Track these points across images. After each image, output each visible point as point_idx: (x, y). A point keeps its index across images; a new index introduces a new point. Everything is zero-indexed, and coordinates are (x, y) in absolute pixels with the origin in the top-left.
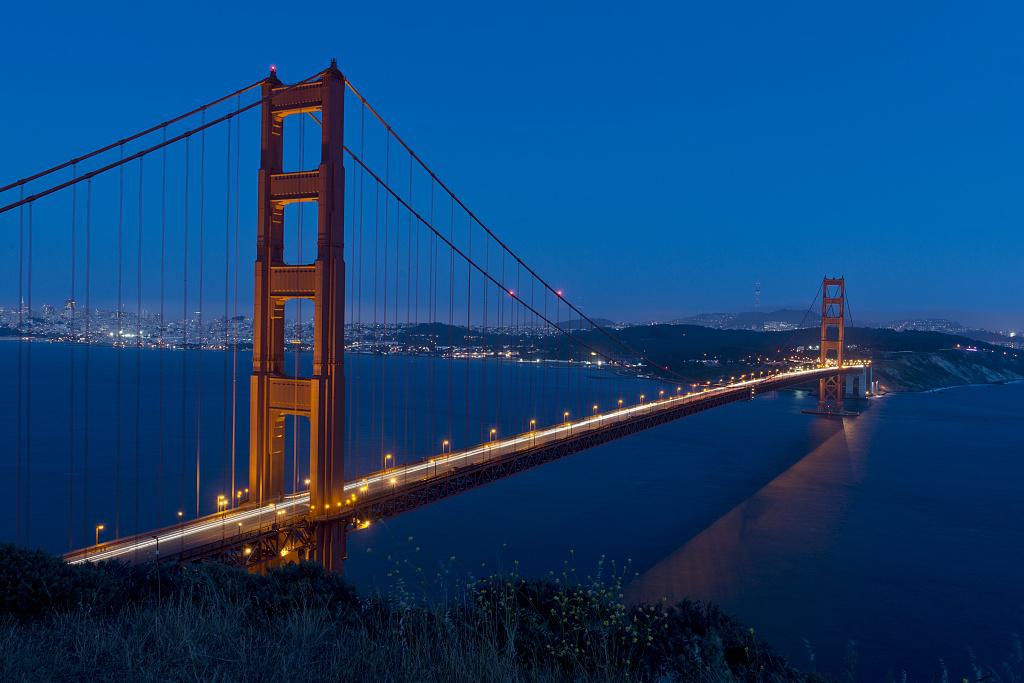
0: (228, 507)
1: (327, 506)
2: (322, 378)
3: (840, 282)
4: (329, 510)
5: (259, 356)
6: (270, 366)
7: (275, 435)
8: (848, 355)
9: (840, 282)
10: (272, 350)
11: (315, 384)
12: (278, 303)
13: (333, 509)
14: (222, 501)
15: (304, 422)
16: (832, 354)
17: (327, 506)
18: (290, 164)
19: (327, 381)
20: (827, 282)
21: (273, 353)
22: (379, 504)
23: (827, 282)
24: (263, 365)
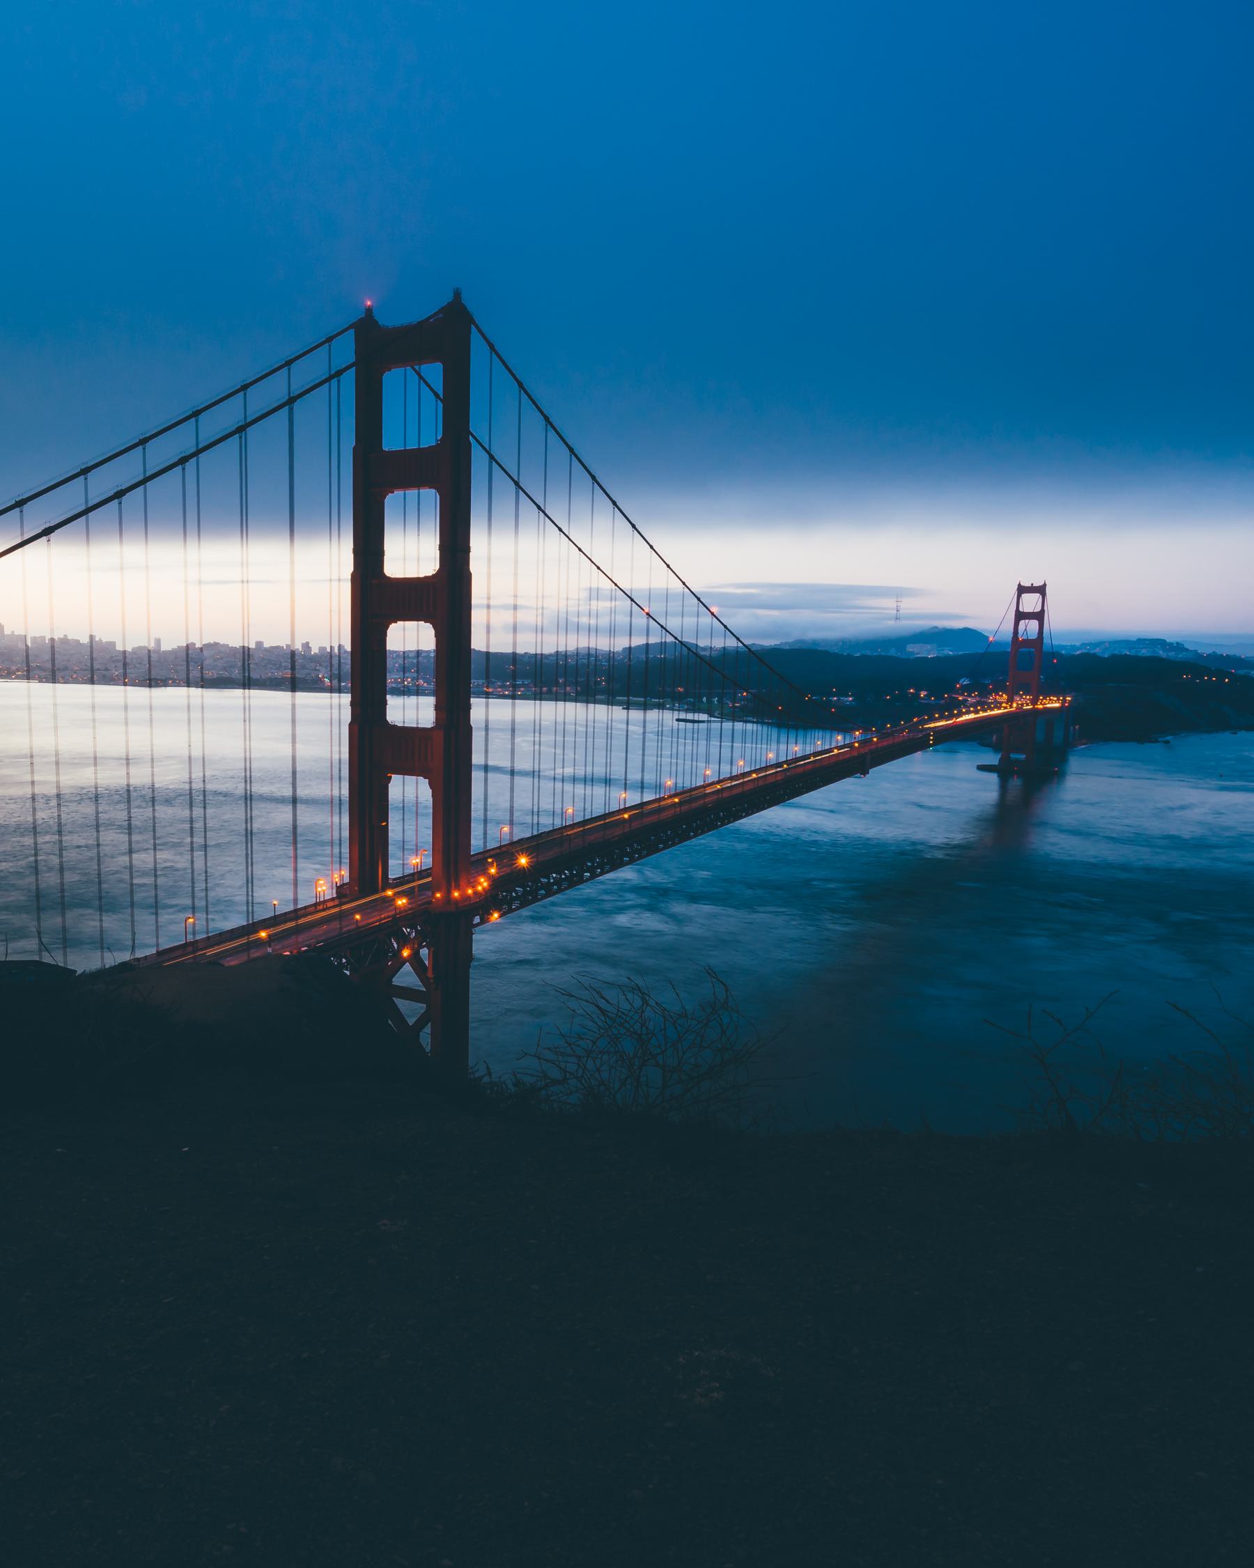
1: (456, 894)
3: (1041, 590)
4: (456, 901)
9: (1041, 590)
13: (465, 897)
18: (392, 441)
20: (1022, 590)
23: (1022, 590)
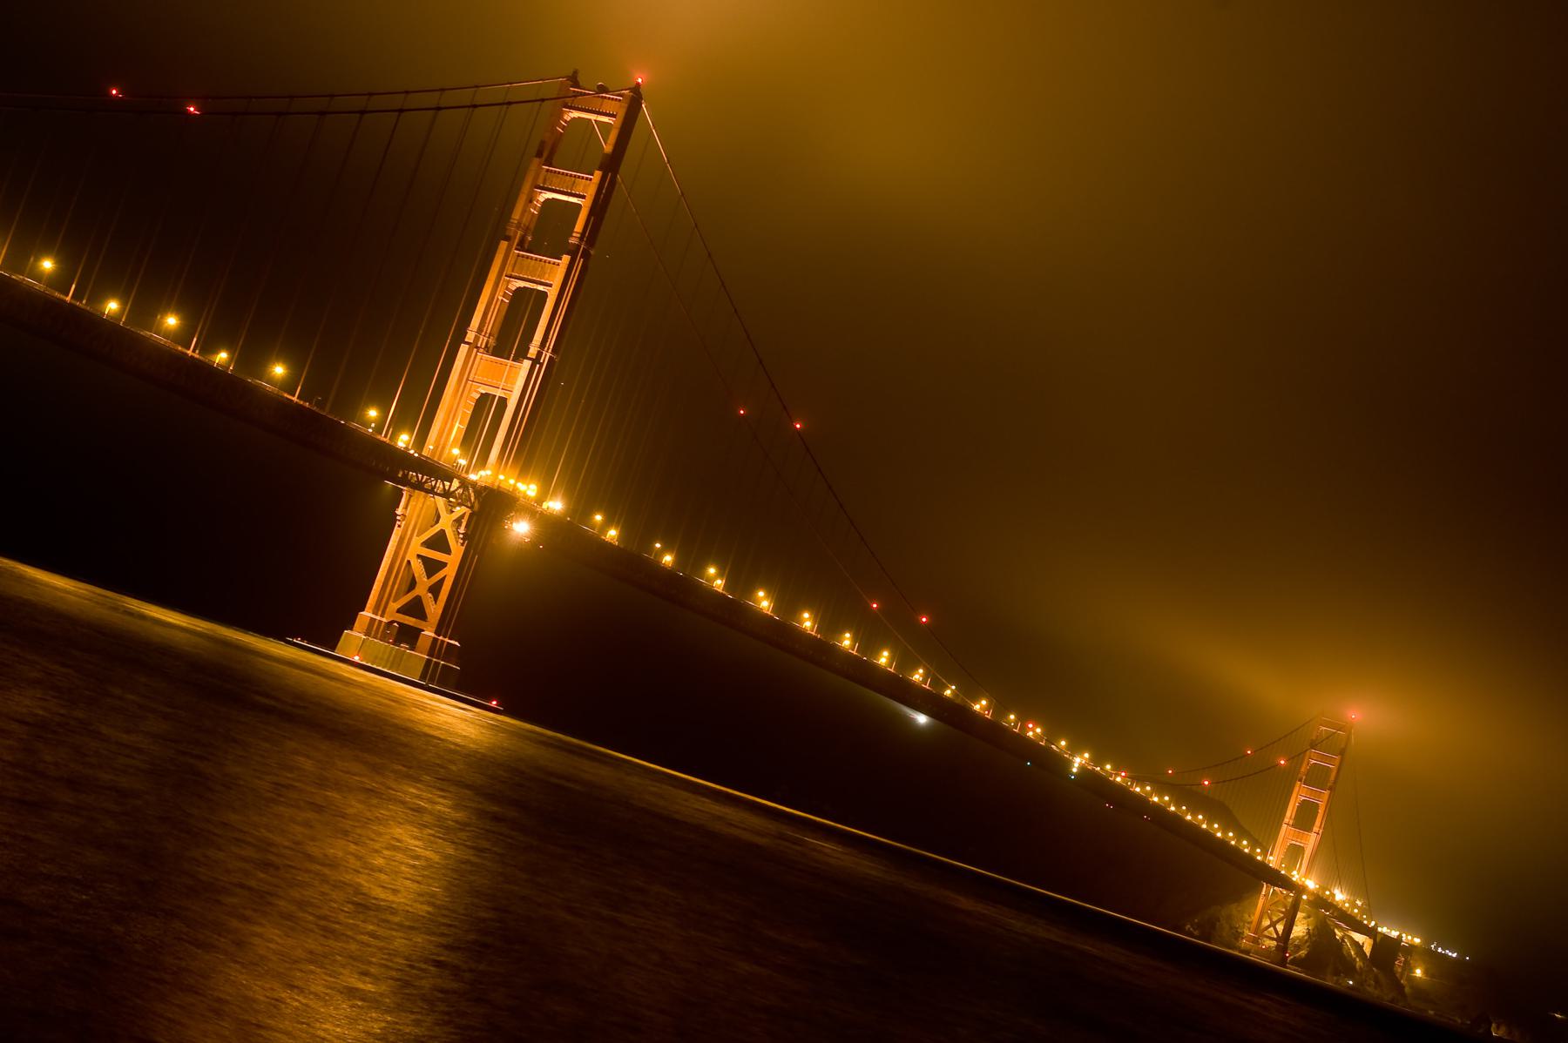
5: (477, 326)
6: (482, 341)
7: (467, 411)
11: (527, 364)
15: (503, 402)
19: (538, 366)
21: (488, 332)
24: (476, 338)
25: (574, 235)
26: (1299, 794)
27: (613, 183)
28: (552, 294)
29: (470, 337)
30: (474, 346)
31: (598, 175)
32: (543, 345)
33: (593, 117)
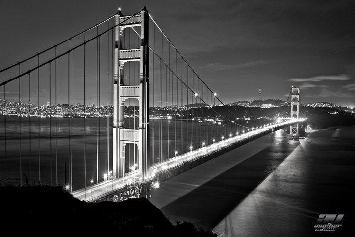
0: (107, 179)
2: (143, 129)
6: (120, 124)
7: (122, 151)
8: (300, 116)
10: (121, 118)
12: (123, 100)
14: (105, 176)
15: (136, 145)
16: (295, 116)
17: (146, 178)
22: (161, 177)
24: (118, 124)
25: (141, 74)
26: (293, 104)
27: (148, 49)
28: (140, 99)
29: (115, 124)
30: (118, 127)
31: (142, 48)
32: (143, 121)
33: (131, 26)
